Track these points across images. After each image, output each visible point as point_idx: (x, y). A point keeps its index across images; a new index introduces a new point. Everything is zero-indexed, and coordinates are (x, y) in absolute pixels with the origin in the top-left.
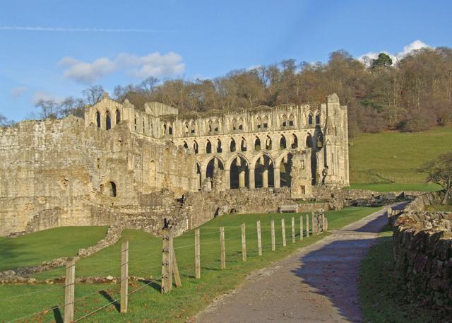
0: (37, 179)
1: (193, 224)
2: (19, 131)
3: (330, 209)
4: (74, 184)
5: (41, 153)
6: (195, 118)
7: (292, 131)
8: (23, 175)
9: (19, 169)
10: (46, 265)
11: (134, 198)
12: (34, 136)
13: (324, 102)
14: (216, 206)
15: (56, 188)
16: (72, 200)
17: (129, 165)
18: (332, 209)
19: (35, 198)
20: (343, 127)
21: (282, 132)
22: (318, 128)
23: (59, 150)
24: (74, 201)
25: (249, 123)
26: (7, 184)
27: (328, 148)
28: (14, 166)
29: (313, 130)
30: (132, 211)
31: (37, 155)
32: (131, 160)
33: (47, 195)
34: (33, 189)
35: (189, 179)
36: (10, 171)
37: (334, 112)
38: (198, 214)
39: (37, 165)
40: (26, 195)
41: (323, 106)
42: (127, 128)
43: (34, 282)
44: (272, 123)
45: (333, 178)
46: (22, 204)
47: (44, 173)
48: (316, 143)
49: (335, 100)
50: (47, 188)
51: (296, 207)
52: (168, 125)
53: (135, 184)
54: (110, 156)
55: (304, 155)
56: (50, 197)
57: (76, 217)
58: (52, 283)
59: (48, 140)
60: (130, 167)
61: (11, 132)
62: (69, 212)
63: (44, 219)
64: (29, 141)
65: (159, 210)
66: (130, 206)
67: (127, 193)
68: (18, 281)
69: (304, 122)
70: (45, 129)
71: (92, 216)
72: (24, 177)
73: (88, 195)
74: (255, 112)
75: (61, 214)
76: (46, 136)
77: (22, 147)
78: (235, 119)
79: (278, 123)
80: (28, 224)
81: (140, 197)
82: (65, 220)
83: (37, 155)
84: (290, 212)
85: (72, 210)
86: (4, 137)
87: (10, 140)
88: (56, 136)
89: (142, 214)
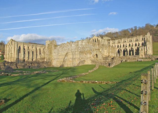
2: (76, 43)
3: (152, 60)
5: (80, 48)
6: (115, 40)
7: (138, 42)
8: (77, 53)
10: (80, 75)
13: (146, 35)
14: (122, 60)
19: (79, 58)
20: (151, 40)
21: (136, 42)
22: (145, 41)
25: (127, 40)
26: (73, 55)
28: (75, 51)
29: (144, 41)
30: (101, 61)
31: (79, 48)
33: (82, 57)
36: (74, 52)
38: (117, 62)
39: (79, 51)
40: (77, 57)
41: (146, 35)
43: (74, 82)
45: (149, 53)
46: (76, 59)
47: (81, 52)
48: (144, 44)
51: (142, 60)
52: (109, 41)
54: (96, 48)
57: (88, 62)
58: (79, 82)
59: (82, 45)
60: (101, 51)
64: (78, 45)
65: (107, 61)
66: (101, 60)
67: (100, 57)
68: (70, 81)
69: (141, 39)
71: (92, 62)
74: (129, 38)
78: (124, 40)
79: (135, 40)
81: (103, 57)
83: (79, 48)
84: (141, 61)
88: (84, 44)
89: (104, 62)
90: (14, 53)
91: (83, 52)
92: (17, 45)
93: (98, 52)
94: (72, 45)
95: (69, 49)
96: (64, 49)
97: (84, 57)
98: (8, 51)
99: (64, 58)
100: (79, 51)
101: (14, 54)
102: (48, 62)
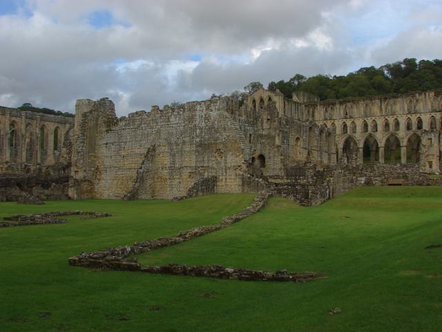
0: (198, 152)
2: (184, 111)
5: (201, 129)
9: (184, 143)
11: (281, 169)
16: (226, 170)
23: (216, 127)
24: (228, 171)
28: (180, 141)
30: (278, 181)
33: (206, 165)
34: (194, 160)
40: (190, 165)
42: (275, 108)
46: (186, 172)
47: (204, 147)
50: (206, 159)
54: (260, 132)
55: (433, 134)
56: (208, 167)
59: (207, 118)
60: (278, 142)
61: (178, 112)
63: (202, 186)
64: (191, 119)
66: (277, 177)
71: (243, 185)
72: (188, 149)
76: (205, 115)
81: (286, 170)
85: (226, 179)
89: (288, 184)
91: (211, 144)
93: (268, 147)
94: (172, 119)
95: (159, 132)
96: (139, 132)
97: (215, 166)
99: (141, 168)
100: (198, 140)
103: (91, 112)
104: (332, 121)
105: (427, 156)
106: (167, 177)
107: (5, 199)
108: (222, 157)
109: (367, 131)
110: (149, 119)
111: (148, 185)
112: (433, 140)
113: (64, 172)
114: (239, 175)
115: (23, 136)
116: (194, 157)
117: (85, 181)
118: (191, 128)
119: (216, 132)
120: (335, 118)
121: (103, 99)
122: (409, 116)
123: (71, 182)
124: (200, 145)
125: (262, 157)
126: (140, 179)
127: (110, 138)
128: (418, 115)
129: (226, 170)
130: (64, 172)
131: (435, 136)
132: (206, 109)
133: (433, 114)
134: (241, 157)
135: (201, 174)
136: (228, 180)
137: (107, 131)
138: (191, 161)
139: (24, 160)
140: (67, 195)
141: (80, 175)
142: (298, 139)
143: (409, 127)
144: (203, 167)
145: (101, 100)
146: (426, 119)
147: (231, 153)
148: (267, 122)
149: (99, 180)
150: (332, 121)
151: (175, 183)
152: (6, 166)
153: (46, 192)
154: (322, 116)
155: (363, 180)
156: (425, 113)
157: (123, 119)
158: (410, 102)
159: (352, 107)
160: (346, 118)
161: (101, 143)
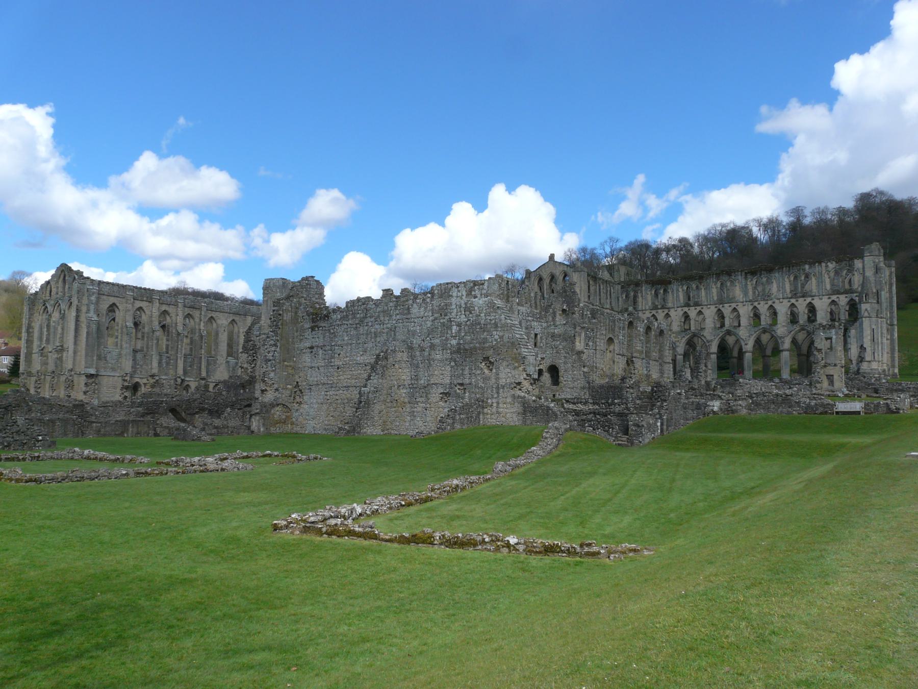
0: (455, 361)
1: (668, 427)
2: (433, 297)
4: (501, 368)
5: (459, 325)
8: (438, 355)
9: (432, 347)
11: (584, 388)
12: (451, 304)
15: (479, 372)
17: (577, 343)
18: (893, 412)
20: (889, 294)
23: (482, 322)
27: (866, 323)
28: (426, 344)
30: (581, 407)
32: (580, 335)
33: (467, 381)
35: (661, 365)
37: (874, 270)
40: (440, 381)
42: (574, 292)
44: (778, 287)
45: (874, 365)
49: (877, 253)
50: (466, 372)
53: (586, 370)
55: (833, 331)
59: (468, 309)
60: (579, 345)
62: (495, 405)
63: (460, 414)
70: (464, 293)
71: (524, 412)
73: (519, 384)
75: (483, 408)
76: (466, 304)
77: (436, 319)
80: (440, 421)
82: (489, 416)
83: (454, 327)
85: (498, 403)
86: (415, 305)
87: (422, 309)
90: (75, 343)
91: (475, 348)
92: (93, 298)
95: (393, 330)
98: (41, 333)
100: (454, 342)
101: (75, 352)
102: (273, 405)
103: (288, 298)
104: (666, 311)
105: (825, 366)
106: (406, 400)
107: (152, 432)
108: (491, 370)
109: (723, 325)
110: (378, 309)
111: (376, 412)
112: (834, 341)
113: (245, 391)
114: (519, 397)
115: (179, 334)
116: (448, 368)
117: (278, 405)
118: (443, 324)
119: (484, 329)
120: (670, 305)
121: (307, 279)
122: (793, 301)
123: (256, 408)
124: (459, 350)
125: (554, 370)
126: (363, 404)
127: (318, 338)
128: (809, 300)
129: (498, 388)
130: (245, 391)
131: (837, 333)
132: (467, 295)
133: (834, 297)
134: (521, 369)
135: (458, 396)
136: (501, 405)
137: (313, 329)
138: (442, 375)
139: (180, 371)
140: (249, 428)
141: (270, 396)
142: (610, 340)
143: (793, 318)
144: (462, 384)
145: (303, 279)
146: (822, 305)
147: (505, 363)
148: (560, 315)
149: (300, 403)
150: (666, 311)
151: (419, 409)
152: (152, 381)
153: (217, 422)
154: (650, 304)
155: (716, 405)
156: (820, 296)
157: (338, 309)
158: (796, 278)
159: (697, 287)
160: (688, 305)
161: (302, 345)
